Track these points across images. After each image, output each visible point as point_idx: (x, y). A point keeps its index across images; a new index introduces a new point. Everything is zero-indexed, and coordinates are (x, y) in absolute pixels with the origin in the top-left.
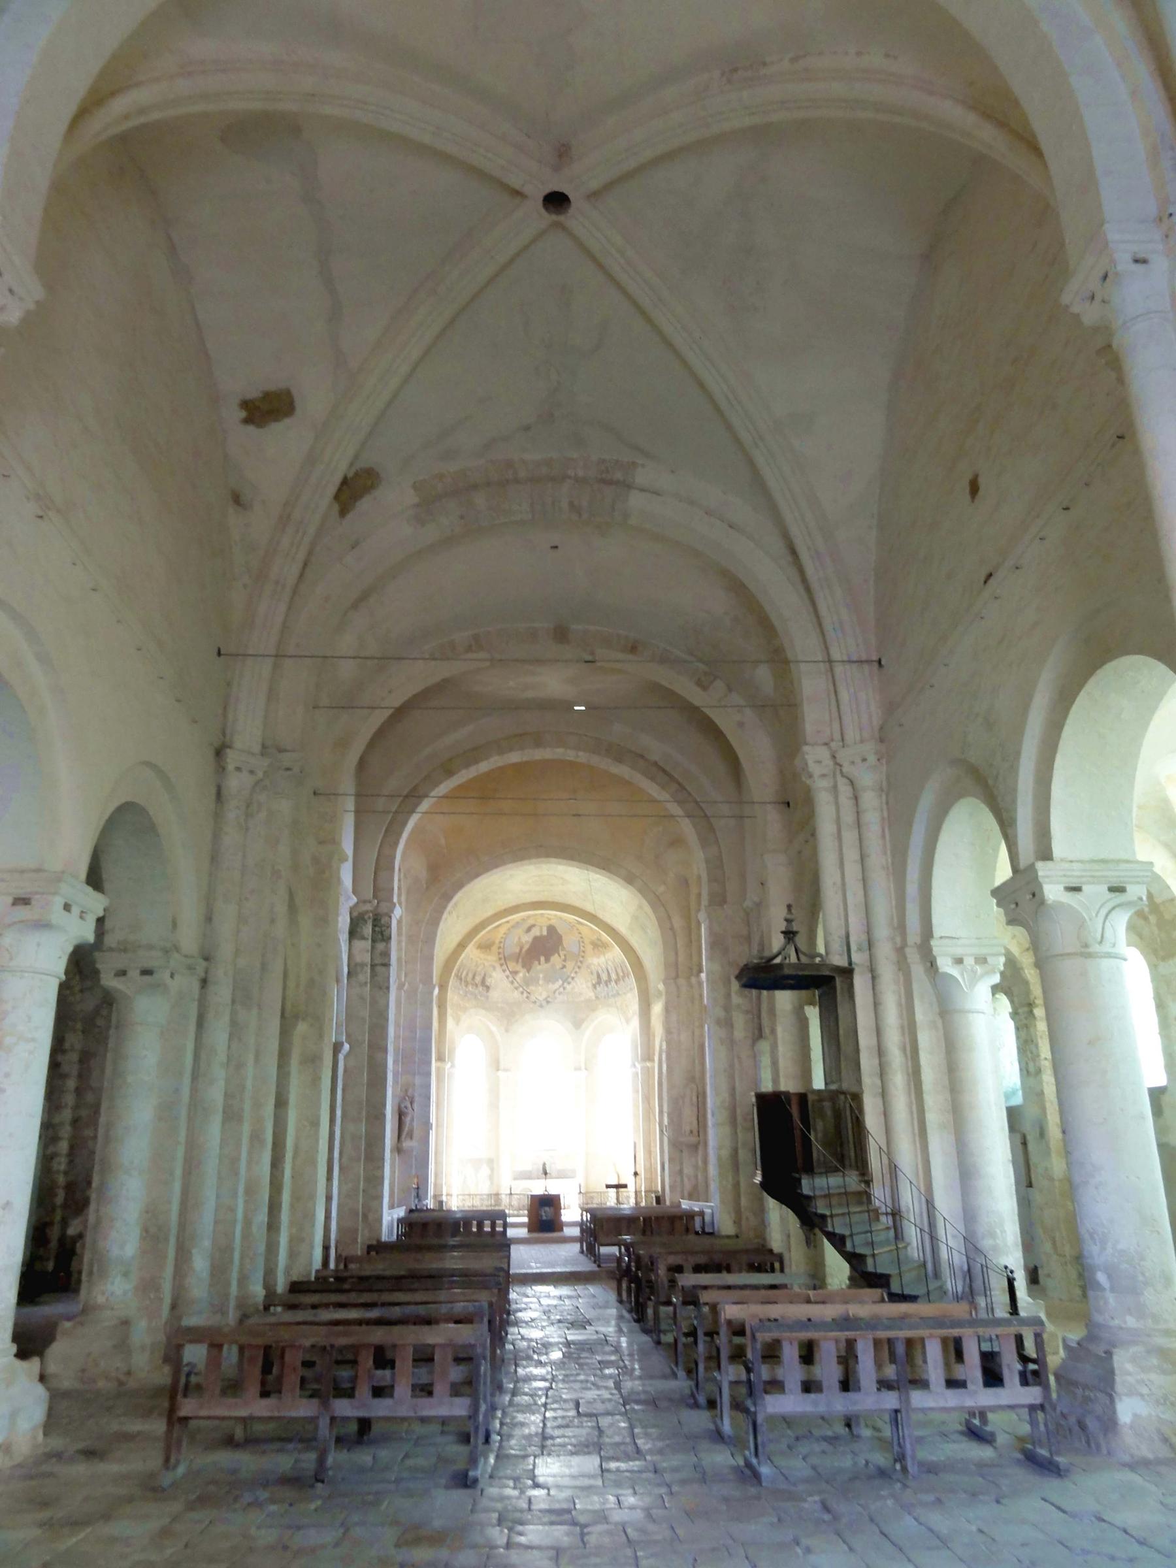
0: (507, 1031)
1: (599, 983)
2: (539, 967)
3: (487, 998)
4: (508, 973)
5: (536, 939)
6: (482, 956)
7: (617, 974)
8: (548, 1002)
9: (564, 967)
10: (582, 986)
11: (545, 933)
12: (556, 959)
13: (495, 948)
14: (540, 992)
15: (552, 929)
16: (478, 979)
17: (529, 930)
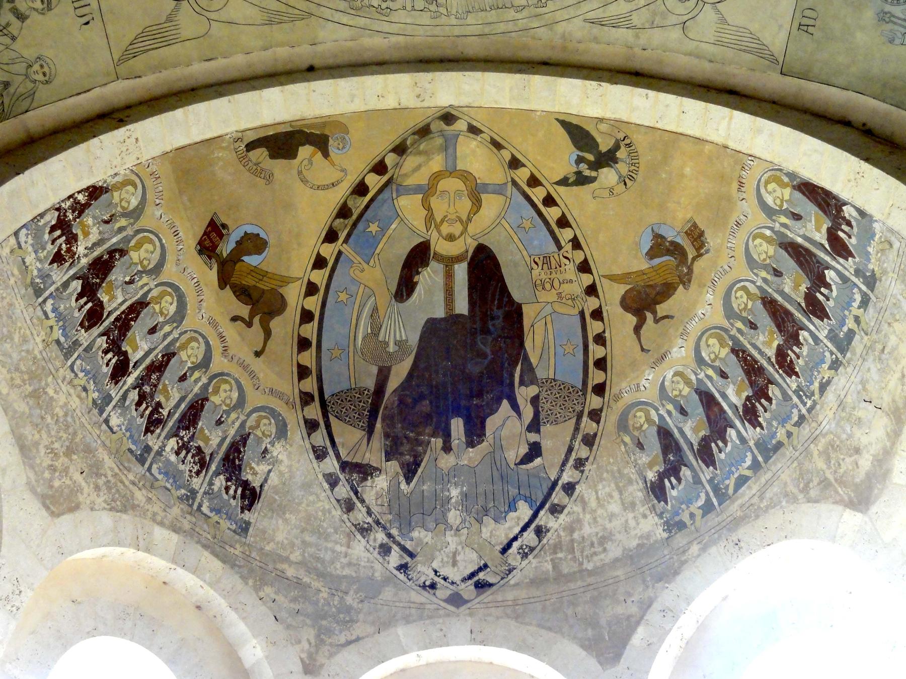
0: (309, 667)
1: (673, 471)
2: (447, 461)
3: (244, 528)
4: (331, 464)
5: (432, 328)
6: (232, 332)
7: (752, 369)
8: (481, 586)
9: (535, 451)
10: (610, 506)
11: (462, 306)
12: (506, 426)
13: (284, 326)
14: (452, 551)
15: (484, 267)
16: (213, 438)
17: (405, 287)
